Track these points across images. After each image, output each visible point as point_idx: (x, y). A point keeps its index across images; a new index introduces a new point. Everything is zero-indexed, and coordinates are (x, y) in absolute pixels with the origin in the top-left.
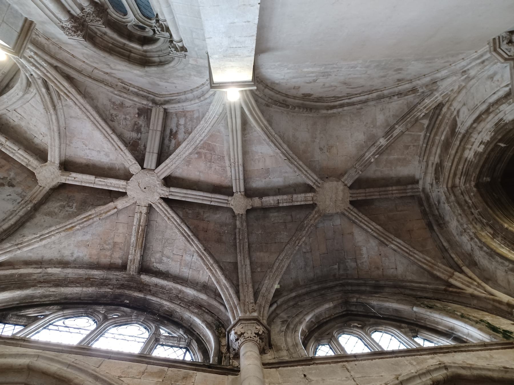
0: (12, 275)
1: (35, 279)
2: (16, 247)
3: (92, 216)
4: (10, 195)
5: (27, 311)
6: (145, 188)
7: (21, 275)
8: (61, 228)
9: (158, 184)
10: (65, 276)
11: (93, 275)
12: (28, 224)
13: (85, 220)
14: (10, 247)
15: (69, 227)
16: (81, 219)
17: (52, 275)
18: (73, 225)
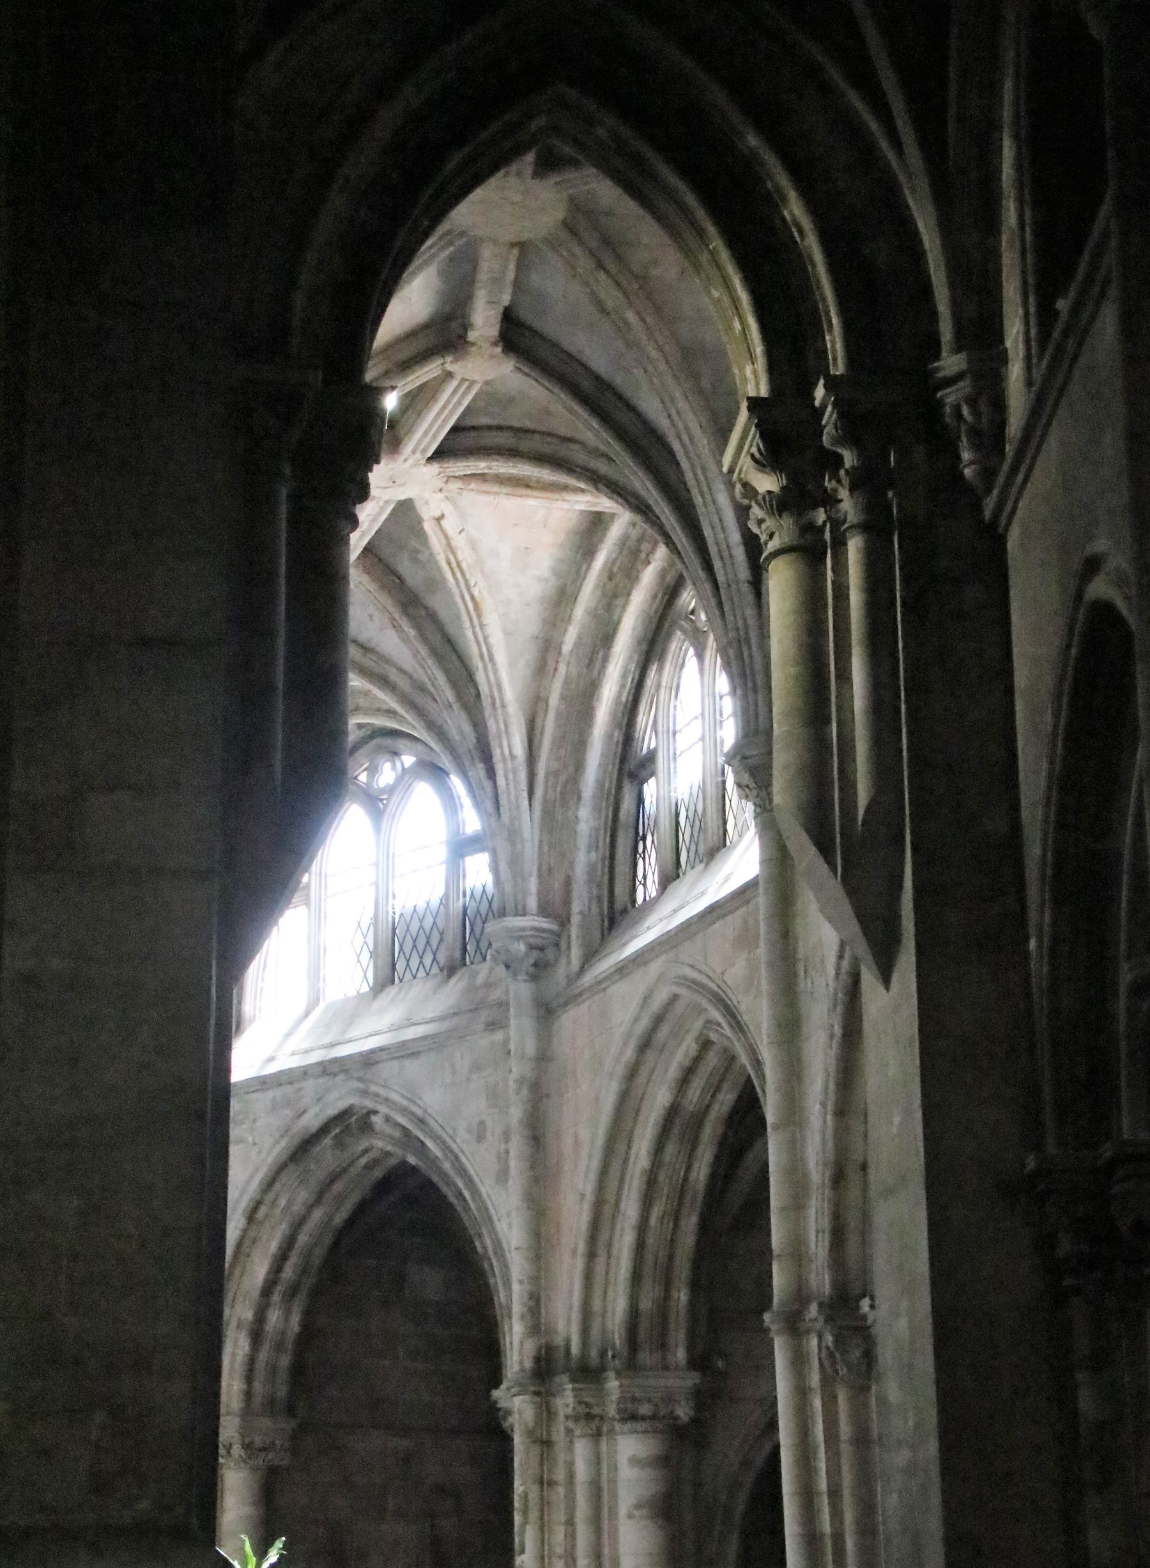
0: (558, 714)
1: (579, 675)
2: (500, 712)
3: (452, 560)
4: (371, 616)
5: (638, 727)
6: (394, 482)
7: (563, 697)
8: (471, 619)
9: (386, 465)
10: (589, 613)
11: (606, 563)
12: (451, 629)
13: (459, 575)
14: (497, 721)
15: (470, 605)
16: (456, 579)
17: (577, 645)
18: (467, 597)
